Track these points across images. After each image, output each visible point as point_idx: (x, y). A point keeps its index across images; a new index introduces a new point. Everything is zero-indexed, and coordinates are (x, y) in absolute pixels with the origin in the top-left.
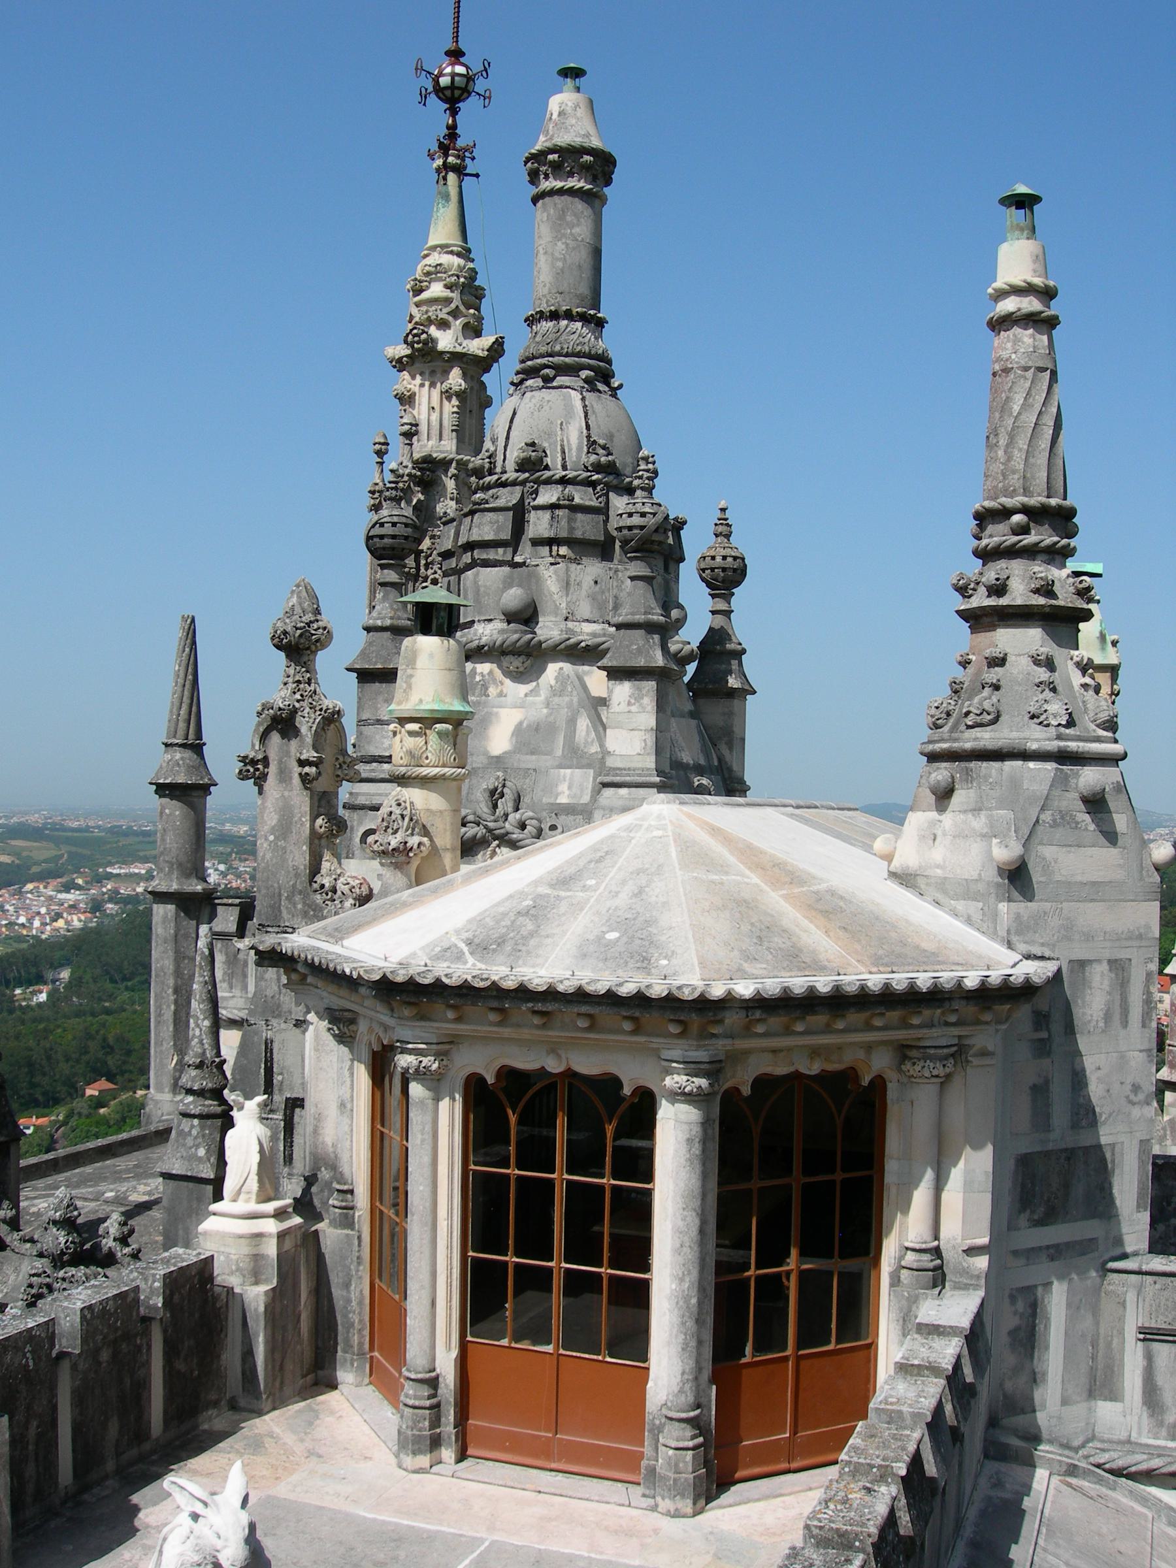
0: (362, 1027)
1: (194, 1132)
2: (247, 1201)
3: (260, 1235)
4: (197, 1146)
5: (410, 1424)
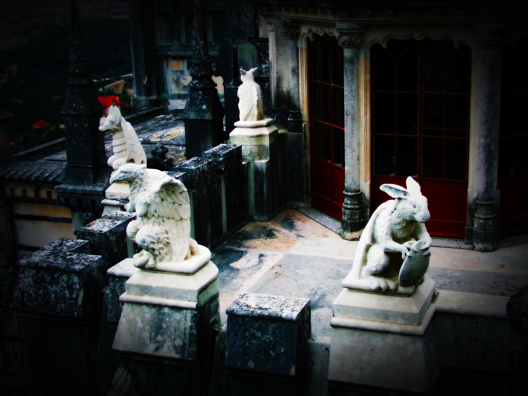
0: (304, 30)
1: (200, 97)
2: (252, 120)
3: (260, 136)
4: (202, 105)
5: (349, 217)
